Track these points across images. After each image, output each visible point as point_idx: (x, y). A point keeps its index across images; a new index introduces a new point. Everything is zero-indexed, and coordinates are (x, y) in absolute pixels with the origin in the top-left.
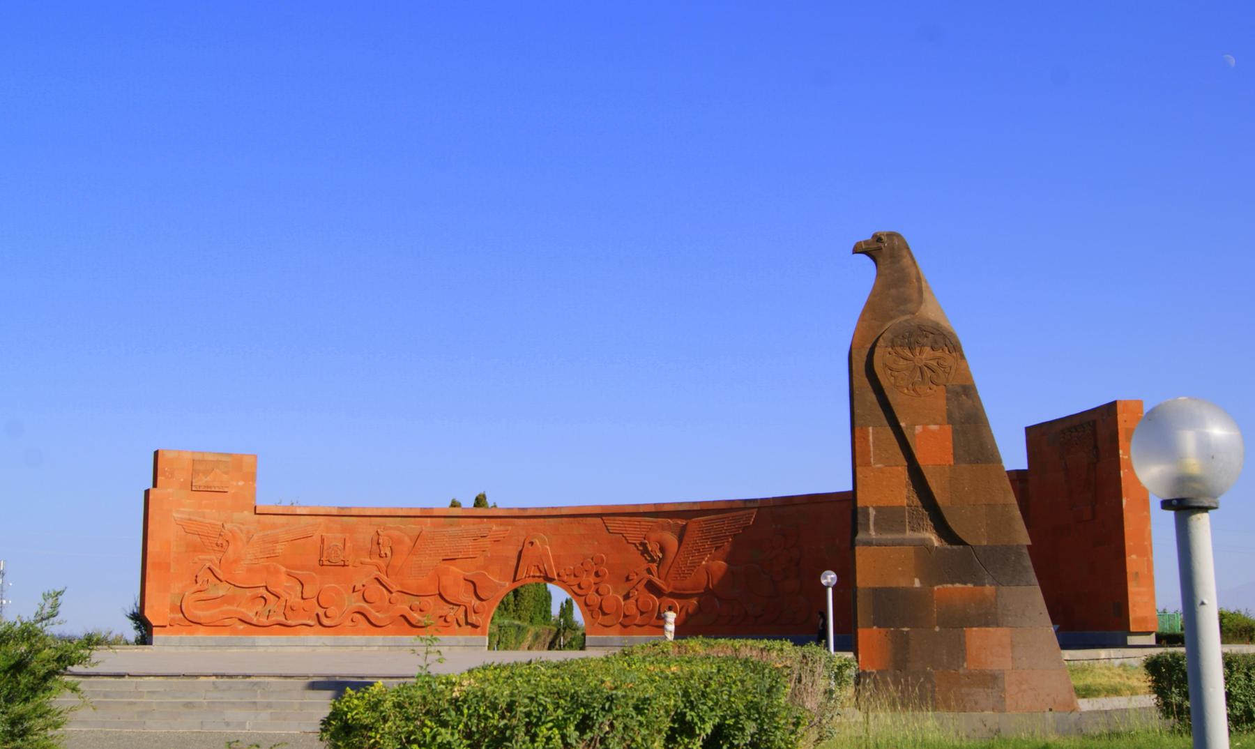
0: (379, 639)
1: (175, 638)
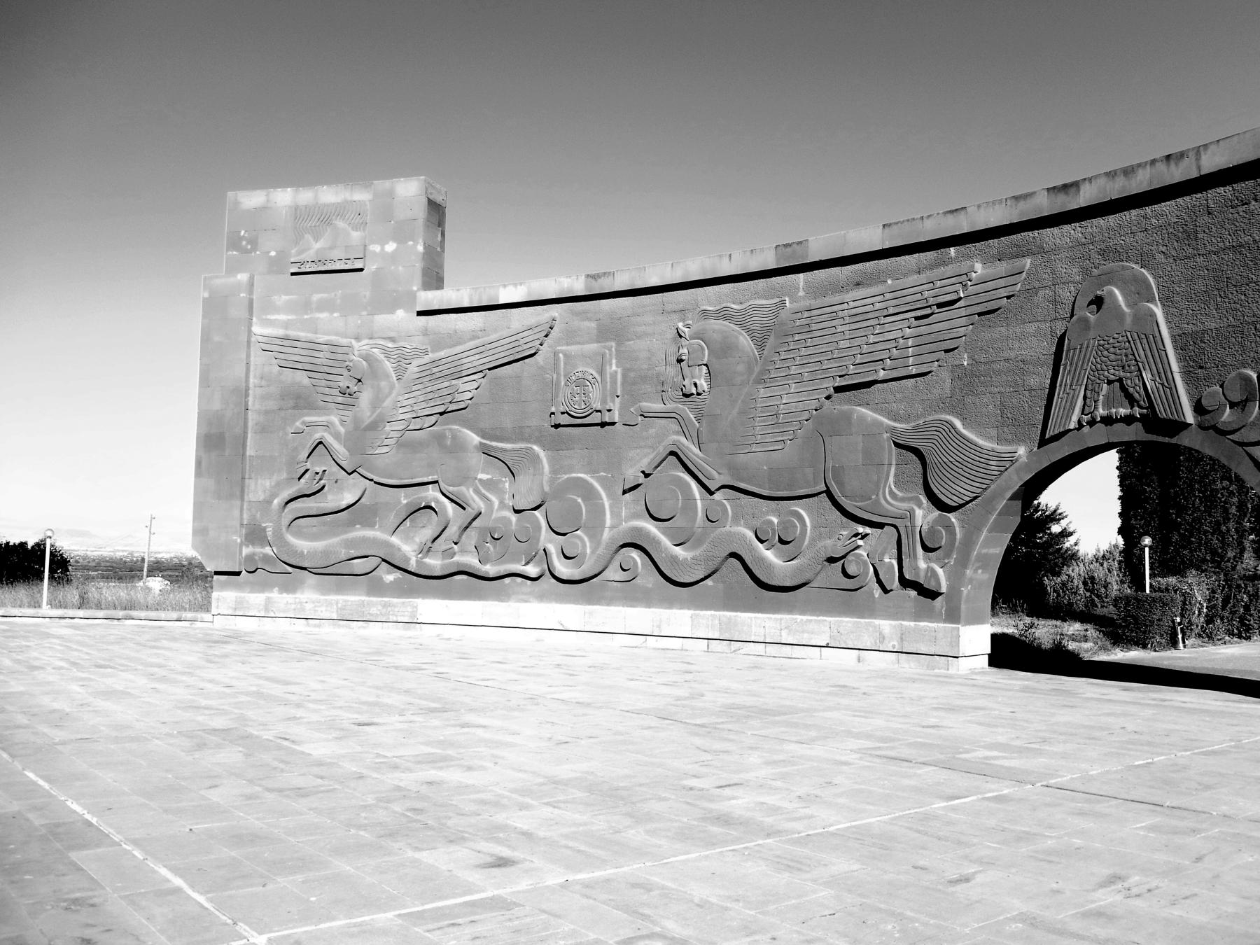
0: (680, 619)
1: (256, 599)
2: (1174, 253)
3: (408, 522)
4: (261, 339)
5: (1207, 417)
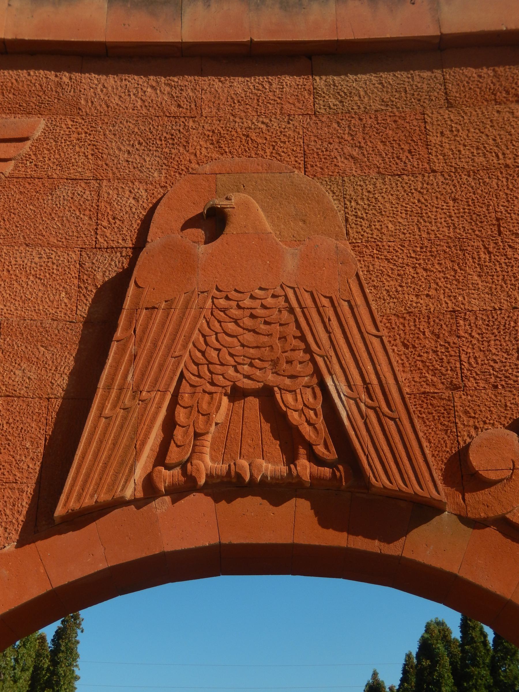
2: (377, 160)
5: (483, 495)
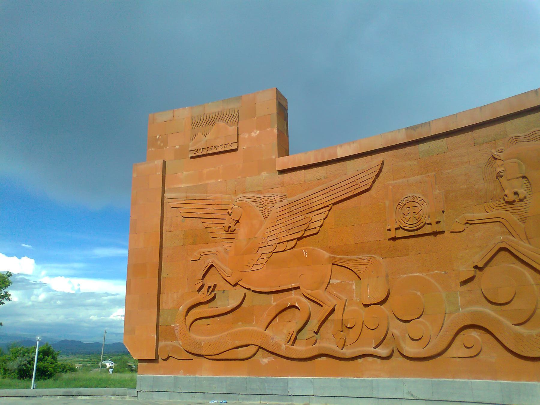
3: (277, 319)
4: (170, 200)
